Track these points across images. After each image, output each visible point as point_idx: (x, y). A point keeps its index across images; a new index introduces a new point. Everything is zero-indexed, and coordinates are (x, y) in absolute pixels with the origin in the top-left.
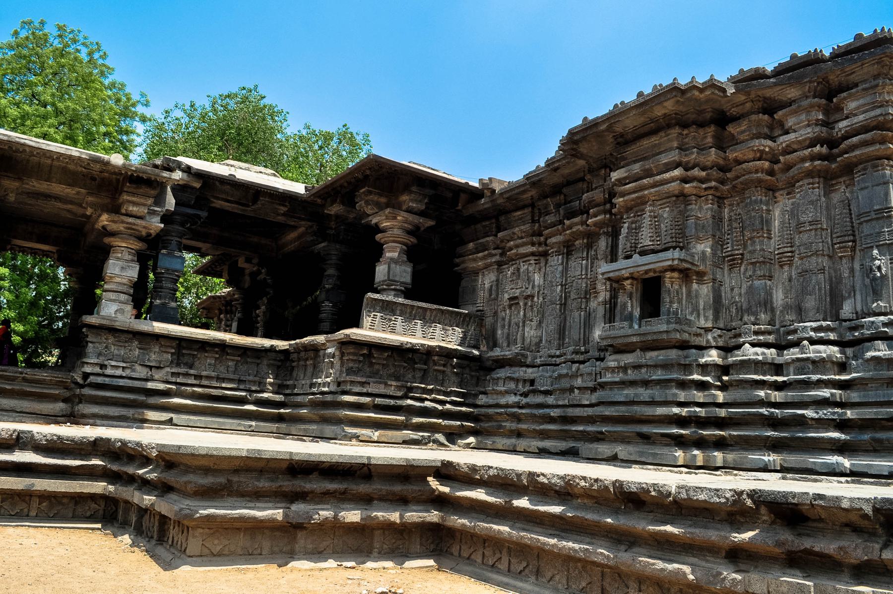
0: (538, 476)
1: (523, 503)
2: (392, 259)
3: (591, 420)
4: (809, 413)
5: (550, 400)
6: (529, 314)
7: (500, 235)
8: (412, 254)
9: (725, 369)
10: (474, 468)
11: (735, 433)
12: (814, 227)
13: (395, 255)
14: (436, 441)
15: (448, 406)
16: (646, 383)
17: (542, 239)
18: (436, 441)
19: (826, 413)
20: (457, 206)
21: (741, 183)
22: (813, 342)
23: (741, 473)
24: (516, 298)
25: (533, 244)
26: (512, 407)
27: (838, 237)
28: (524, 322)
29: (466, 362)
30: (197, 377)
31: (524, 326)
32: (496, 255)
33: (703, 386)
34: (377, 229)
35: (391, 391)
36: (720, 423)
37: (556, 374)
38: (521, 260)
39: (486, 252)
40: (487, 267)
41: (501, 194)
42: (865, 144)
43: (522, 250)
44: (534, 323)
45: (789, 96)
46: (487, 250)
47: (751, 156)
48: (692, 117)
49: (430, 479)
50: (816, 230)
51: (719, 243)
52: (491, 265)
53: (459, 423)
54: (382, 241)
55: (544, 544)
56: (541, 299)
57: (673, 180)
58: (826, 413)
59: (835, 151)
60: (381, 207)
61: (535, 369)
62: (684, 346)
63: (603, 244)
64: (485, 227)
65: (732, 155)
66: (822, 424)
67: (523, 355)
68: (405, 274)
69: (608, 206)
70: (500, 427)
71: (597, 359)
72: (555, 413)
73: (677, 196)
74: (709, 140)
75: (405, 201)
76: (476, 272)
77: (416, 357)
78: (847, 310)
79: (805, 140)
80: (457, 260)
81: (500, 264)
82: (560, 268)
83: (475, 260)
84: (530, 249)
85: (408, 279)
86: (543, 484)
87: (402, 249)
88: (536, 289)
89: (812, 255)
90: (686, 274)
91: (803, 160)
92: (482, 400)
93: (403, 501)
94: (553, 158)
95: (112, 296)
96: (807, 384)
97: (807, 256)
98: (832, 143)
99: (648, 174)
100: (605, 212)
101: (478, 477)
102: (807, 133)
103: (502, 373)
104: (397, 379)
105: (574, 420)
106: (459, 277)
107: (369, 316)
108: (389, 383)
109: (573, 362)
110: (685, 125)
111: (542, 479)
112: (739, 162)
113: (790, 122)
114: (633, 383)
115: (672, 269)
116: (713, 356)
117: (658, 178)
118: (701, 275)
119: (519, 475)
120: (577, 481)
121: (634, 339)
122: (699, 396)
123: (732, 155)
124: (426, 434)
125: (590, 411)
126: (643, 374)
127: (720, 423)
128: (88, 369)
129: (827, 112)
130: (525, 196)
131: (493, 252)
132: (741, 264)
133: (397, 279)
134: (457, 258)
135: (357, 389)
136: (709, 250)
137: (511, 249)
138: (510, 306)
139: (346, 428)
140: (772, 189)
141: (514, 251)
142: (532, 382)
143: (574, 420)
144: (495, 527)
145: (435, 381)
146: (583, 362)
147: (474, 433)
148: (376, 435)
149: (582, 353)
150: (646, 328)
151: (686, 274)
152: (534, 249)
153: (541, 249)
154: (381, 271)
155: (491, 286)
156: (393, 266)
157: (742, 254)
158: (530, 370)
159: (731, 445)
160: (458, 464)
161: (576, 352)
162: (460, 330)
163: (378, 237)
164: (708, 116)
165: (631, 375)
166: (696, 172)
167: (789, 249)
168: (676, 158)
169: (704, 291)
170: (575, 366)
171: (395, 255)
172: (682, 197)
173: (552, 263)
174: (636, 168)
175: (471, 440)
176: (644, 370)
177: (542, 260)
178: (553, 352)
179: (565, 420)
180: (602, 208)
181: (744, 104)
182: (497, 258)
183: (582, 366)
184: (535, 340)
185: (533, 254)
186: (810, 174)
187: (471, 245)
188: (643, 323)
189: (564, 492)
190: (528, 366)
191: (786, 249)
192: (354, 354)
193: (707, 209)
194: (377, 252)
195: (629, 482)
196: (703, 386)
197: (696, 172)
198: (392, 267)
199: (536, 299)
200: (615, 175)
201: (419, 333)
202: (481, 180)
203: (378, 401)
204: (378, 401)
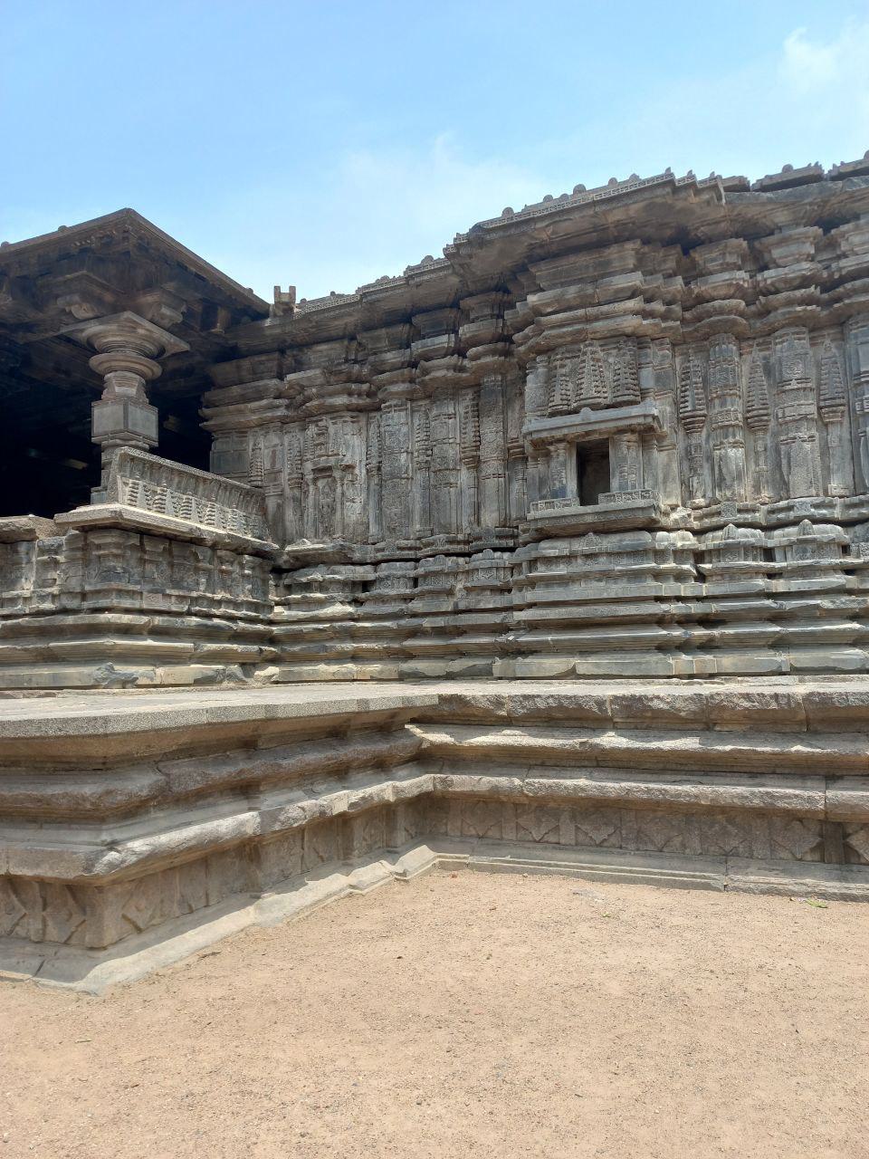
0: (652, 699)
1: (611, 740)
2: (126, 401)
3: (504, 629)
5: (417, 606)
6: (350, 493)
7: (290, 377)
8: (156, 393)
10: (498, 701)
11: (731, 631)
12: (804, 385)
14: (231, 677)
15: (241, 624)
16: (606, 576)
17: (365, 387)
18: (231, 677)
19: (844, 602)
20: (215, 327)
21: (710, 325)
22: (815, 521)
23: (746, 679)
24: (330, 469)
25: (350, 394)
27: (825, 400)
28: (342, 504)
29: (258, 560)
31: (342, 509)
32: (278, 407)
34: (90, 349)
36: (706, 621)
37: (421, 571)
38: (329, 416)
39: (264, 402)
40: (263, 425)
41: (306, 317)
44: (358, 507)
45: (777, 220)
46: (261, 398)
47: (723, 292)
48: (650, 231)
49: (406, 726)
50: (805, 389)
52: (271, 420)
53: (256, 648)
54: (100, 369)
55: (679, 795)
56: (364, 471)
57: (625, 313)
59: (826, 296)
60: (109, 311)
61: (368, 568)
62: (652, 527)
64: (261, 363)
65: (696, 288)
67: (350, 548)
68: (146, 421)
69: (500, 345)
70: (325, 648)
71: (495, 550)
72: (427, 623)
73: (628, 336)
74: (670, 264)
75: (151, 305)
76: (243, 431)
77: (203, 553)
79: (795, 278)
80: (207, 412)
81: (284, 421)
82: (405, 429)
83: (241, 412)
84: (341, 400)
85: (153, 432)
86: (661, 710)
87: (140, 383)
88: (357, 458)
89: (799, 420)
90: (647, 435)
91: (790, 303)
93: (381, 766)
94: (418, 267)
97: (795, 421)
100: (494, 353)
101: (504, 713)
103: (317, 575)
104: (177, 584)
107: (126, 484)
108: (168, 592)
109: (448, 555)
110: (646, 242)
111: (656, 704)
112: (701, 300)
115: (631, 429)
117: (605, 308)
119: (600, 703)
120: (735, 700)
121: (589, 519)
123: (696, 288)
124: (220, 667)
125: (496, 619)
126: (602, 564)
127: (706, 621)
130: (336, 323)
131: (278, 402)
132: (702, 427)
133: (138, 430)
134: (207, 407)
135: (127, 603)
136: (668, 409)
137: (309, 399)
138: (315, 480)
139: (116, 667)
140: (740, 338)
141: (315, 403)
142: (366, 585)
143: (460, 631)
144: (569, 782)
145: (226, 588)
146: (469, 555)
147: (274, 661)
148: (161, 672)
149: (459, 543)
150: (604, 504)
151: (647, 435)
152: (355, 400)
153: (361, 402)
154: (104, 418)
155: (274, 452)
156: (131, 408)
157: (704, 416)
158: (360, 569)
159: (717, 647)
160: (474, 697)
161: (451, 542)
162: (242, 514)
163: (95, 361)
164: (668, 233)
166: (658, 306)
167: (765, 412)
168: (638, 283)
170: (450, 561)
171: (132, 391)
173: (390, 422)
175: (272, 670)
176: (603, 559)
177: (363, 419)
178: (403, 543)
179: (440, 632)
180: (492, 346)
181: (718, 223)
182: (280, 412)
183: (461, 560)
184: (361, 529)
185: (348, 408)
186: (797, 321)
187: (236, 390)
188: (601, 496)
189: (707, 718)
190: (353, 564)
191: (761, 412)
192: (118, 546)
193: (663, 356)
195: (841, 694)
196: (680, 577)
197: (658, 306)
198: (121, 413)
199: (357, 471)
201: (194, 515)
202: (277, 289)
203: (158, 620)
204: (158, 620)
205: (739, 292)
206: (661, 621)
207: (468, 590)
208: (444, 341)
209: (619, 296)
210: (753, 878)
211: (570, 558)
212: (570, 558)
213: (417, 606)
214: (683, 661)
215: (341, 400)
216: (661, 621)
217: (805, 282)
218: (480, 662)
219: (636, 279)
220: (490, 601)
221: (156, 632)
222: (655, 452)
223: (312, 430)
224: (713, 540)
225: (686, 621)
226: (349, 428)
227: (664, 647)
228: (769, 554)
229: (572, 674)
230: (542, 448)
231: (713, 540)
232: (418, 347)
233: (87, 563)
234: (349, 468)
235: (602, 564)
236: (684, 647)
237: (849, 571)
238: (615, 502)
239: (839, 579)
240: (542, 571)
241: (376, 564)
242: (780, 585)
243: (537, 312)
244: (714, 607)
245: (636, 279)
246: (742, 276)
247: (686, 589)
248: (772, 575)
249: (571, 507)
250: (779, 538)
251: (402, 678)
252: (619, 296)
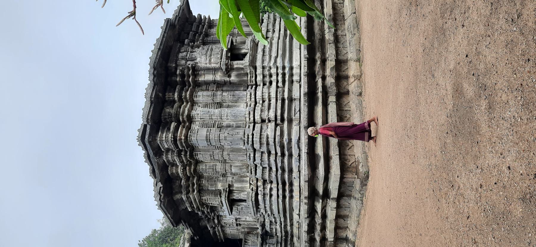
4: (279, 165)
26: (281, 228)
28: (247, 221)
33: (271, 189)
40: (223, 231)
52: (222, 230)
92: (279, 234)
106: (227, 239)
118: (230, 186)
122: (274, 192)
196: (271, 189)
197: (191, 190)
205: (184, 169)
206: (284, 197)
209: (188, 198)
216: (284, 197)
222: (234, 189)
225: (284, 190)
229: (299, 215)
234: (236, 220)
236: (291, 191)
237: (269, 153)
239: (272, 158)
252: (188, 198)
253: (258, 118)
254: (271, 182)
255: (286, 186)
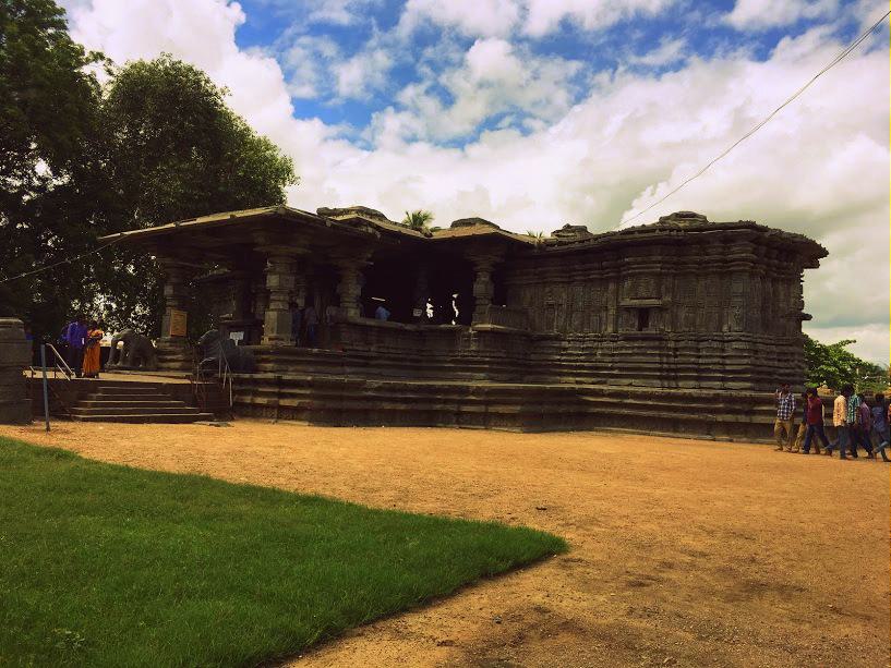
3: (612, 369)
5: (582, 358)
8: (494, 277)
9: (676, 349)
13: (487, 279)
16: (643, 354)
19: (718, 367)
25: (561, 277)
30: (388, 348)
35: (501, 355)
42: (738, 265)
43: (556, 279)
51: (674, 297)
58: (718, 367)
62: (660, 339)
63: (612, 287)
66: (715, 371)
78: (725, 328)
84: (559, 279)
90: (661, 309)
95: (351, 305)
96: (711, 356)
98: (726, 262)
99: (645, 262)
102: (717, 257)
103: (550, 343)
105: (597, 368)
112: (685, 263)
113: (710, 251)
114: (637, 354)
116: (671, 345)
126: (643, 351)
128: (347, 347)
129: (724, 248)
147: (530, 373)
165: (636, 350)
169: (667, 316)
170: (596, 344)
172: (661, 274)
174: (639, 259)
185: (563, 282)
194: (473, 277)
200: (626, 260)
203: (500, 360)
204: (500, 360)
205: (696, 263)
207: (602, 355)
208: (596, 265)
209: (655, 262)
210: (657, 433)
211: (633, 348)
212: (633, 348)
213: (582, 358)
214: (666, 384)
215: (559, 279)
216: (659, 370)
217: (717, 261)
218: (604, 379)
219: (660, 258)
220: (610, 359)
221: (498, 363)
223: (547, 290)
224: (682, 344)
226: (562, 290)
227: (659, 378)
228: (698, 350)
229: (630, 385)
230: (628, 309)
231: (682, 344)
232: (588, 265)
233: (479, 341)
235: (643, 351)
236: (667, 378)
237: (723, 357)
238: (651, 331)
240: (624, 351)
241: (569, 341)
242: (701, 361)
243: (628, 263)
244: (679, 366)
245: (660, 258)
246: (697, 258)
247: (672, 359)
248: (699, 357)
249: (634, 331)
250: (702, 345)
251: (577, 382)
252: (655, 262)
253: (761, 347)
254: (676, 356)
255: (670, 374)
